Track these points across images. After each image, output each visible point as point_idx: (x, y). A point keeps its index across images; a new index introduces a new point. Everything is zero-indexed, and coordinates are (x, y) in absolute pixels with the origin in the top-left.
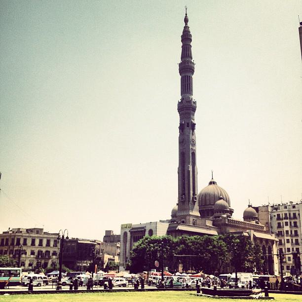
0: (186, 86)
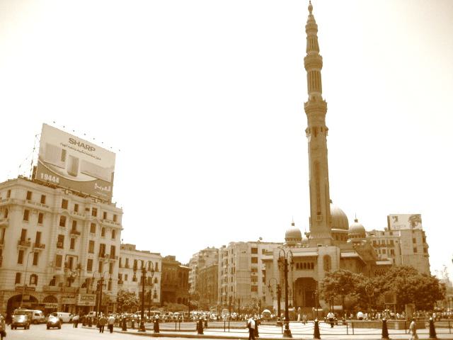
0: (315, 82)
